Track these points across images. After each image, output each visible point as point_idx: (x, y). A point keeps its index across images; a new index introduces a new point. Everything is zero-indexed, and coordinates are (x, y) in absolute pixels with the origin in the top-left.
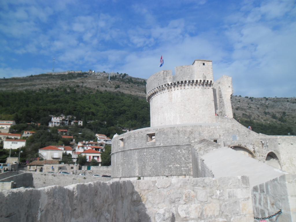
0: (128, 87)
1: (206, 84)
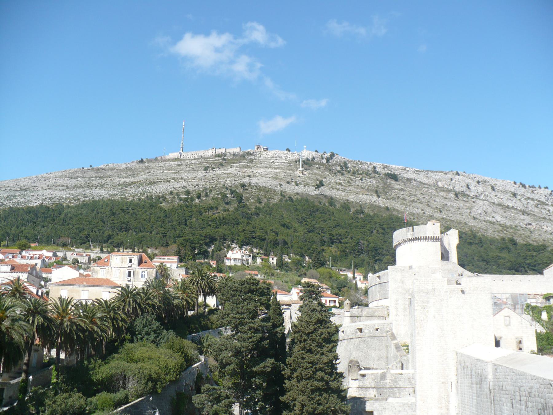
0: (340, 184)
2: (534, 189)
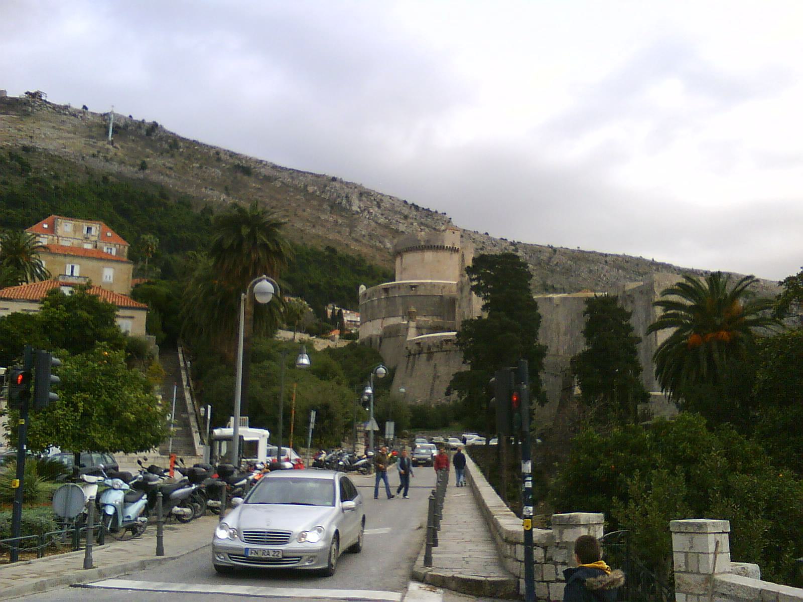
0: (171, 168)
1: (454, 250)
2: (430, 213)
